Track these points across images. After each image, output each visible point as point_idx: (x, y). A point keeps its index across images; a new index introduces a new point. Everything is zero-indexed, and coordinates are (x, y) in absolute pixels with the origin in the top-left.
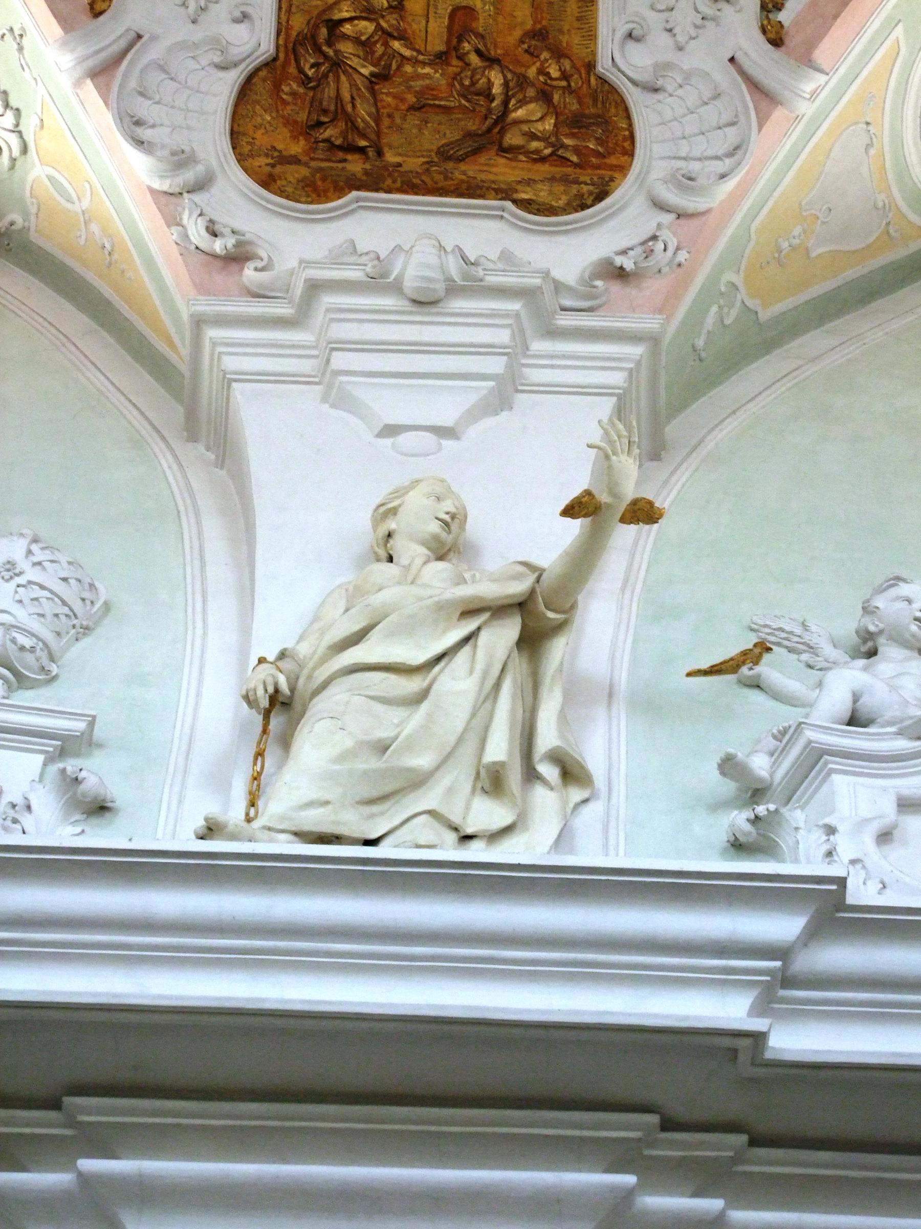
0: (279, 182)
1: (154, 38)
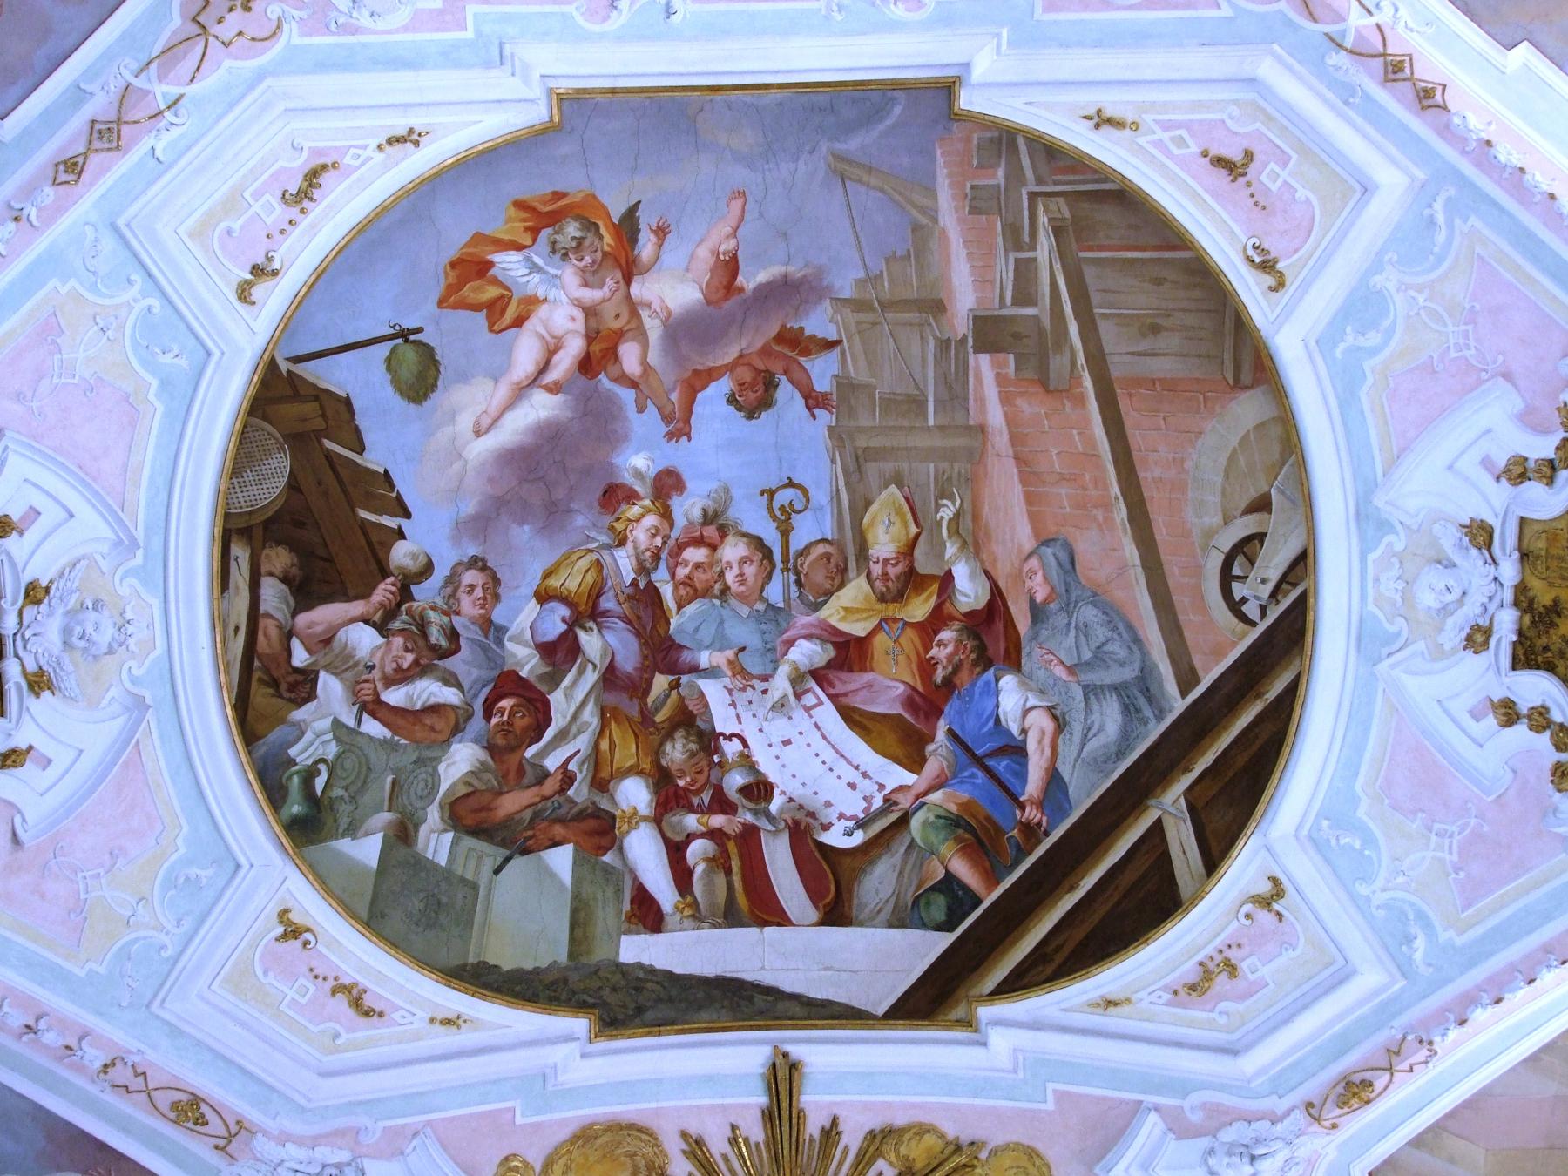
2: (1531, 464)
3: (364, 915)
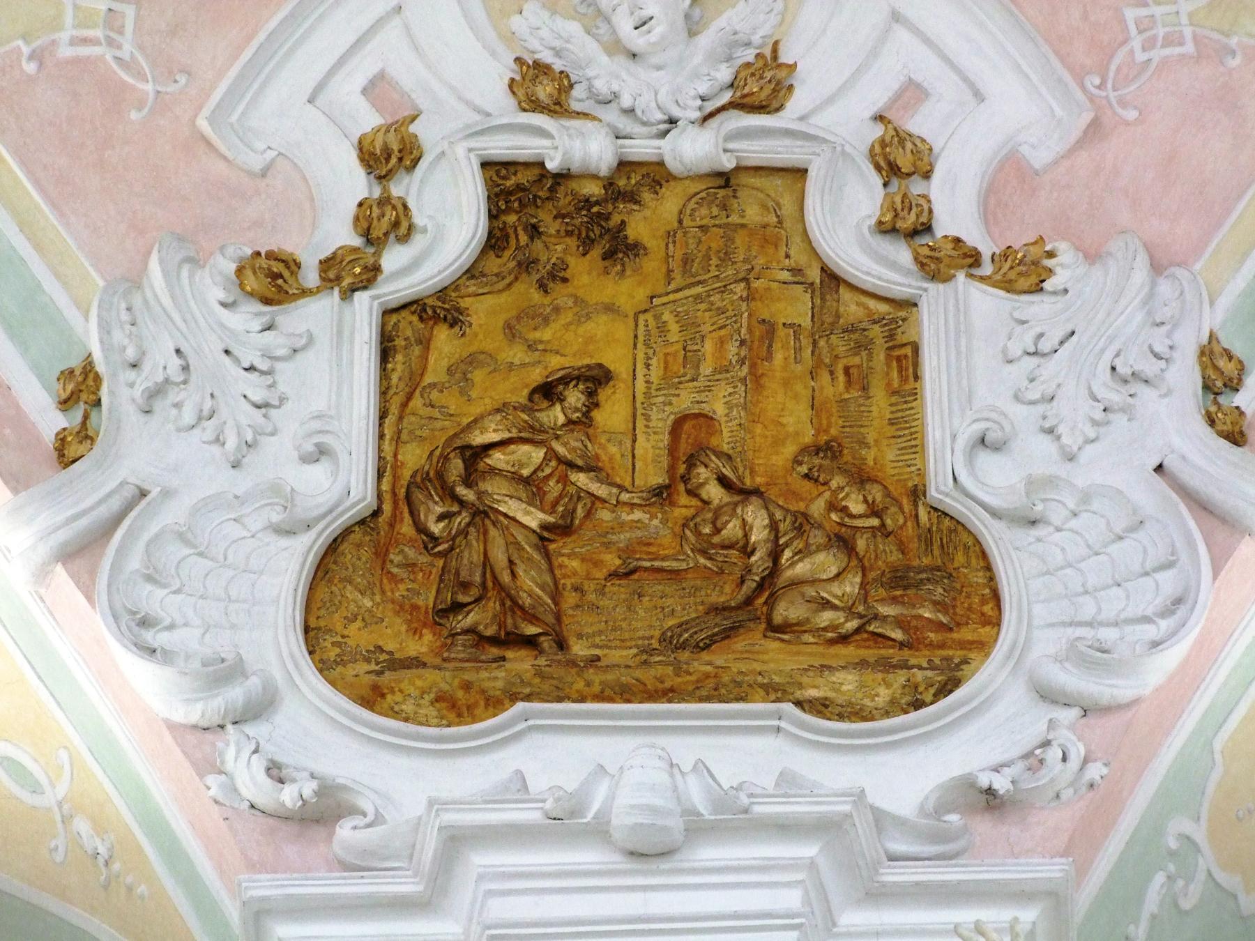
0: (389, 697)
1: (167, 494)
2: (916, 187)
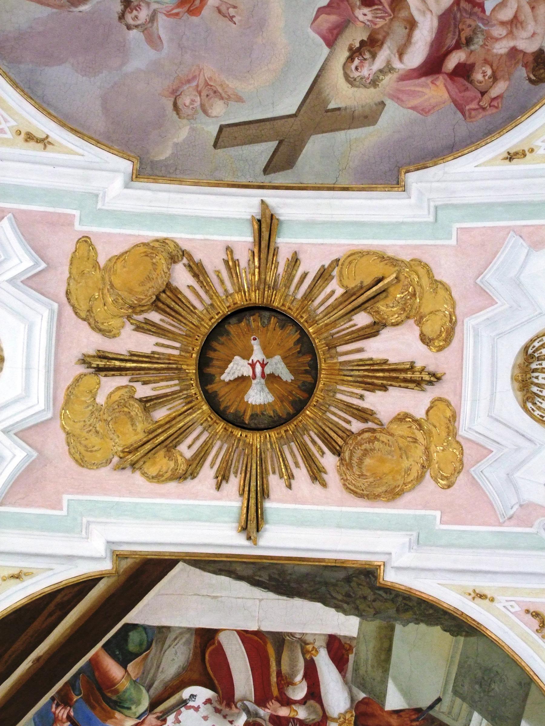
3: (533, 687)
